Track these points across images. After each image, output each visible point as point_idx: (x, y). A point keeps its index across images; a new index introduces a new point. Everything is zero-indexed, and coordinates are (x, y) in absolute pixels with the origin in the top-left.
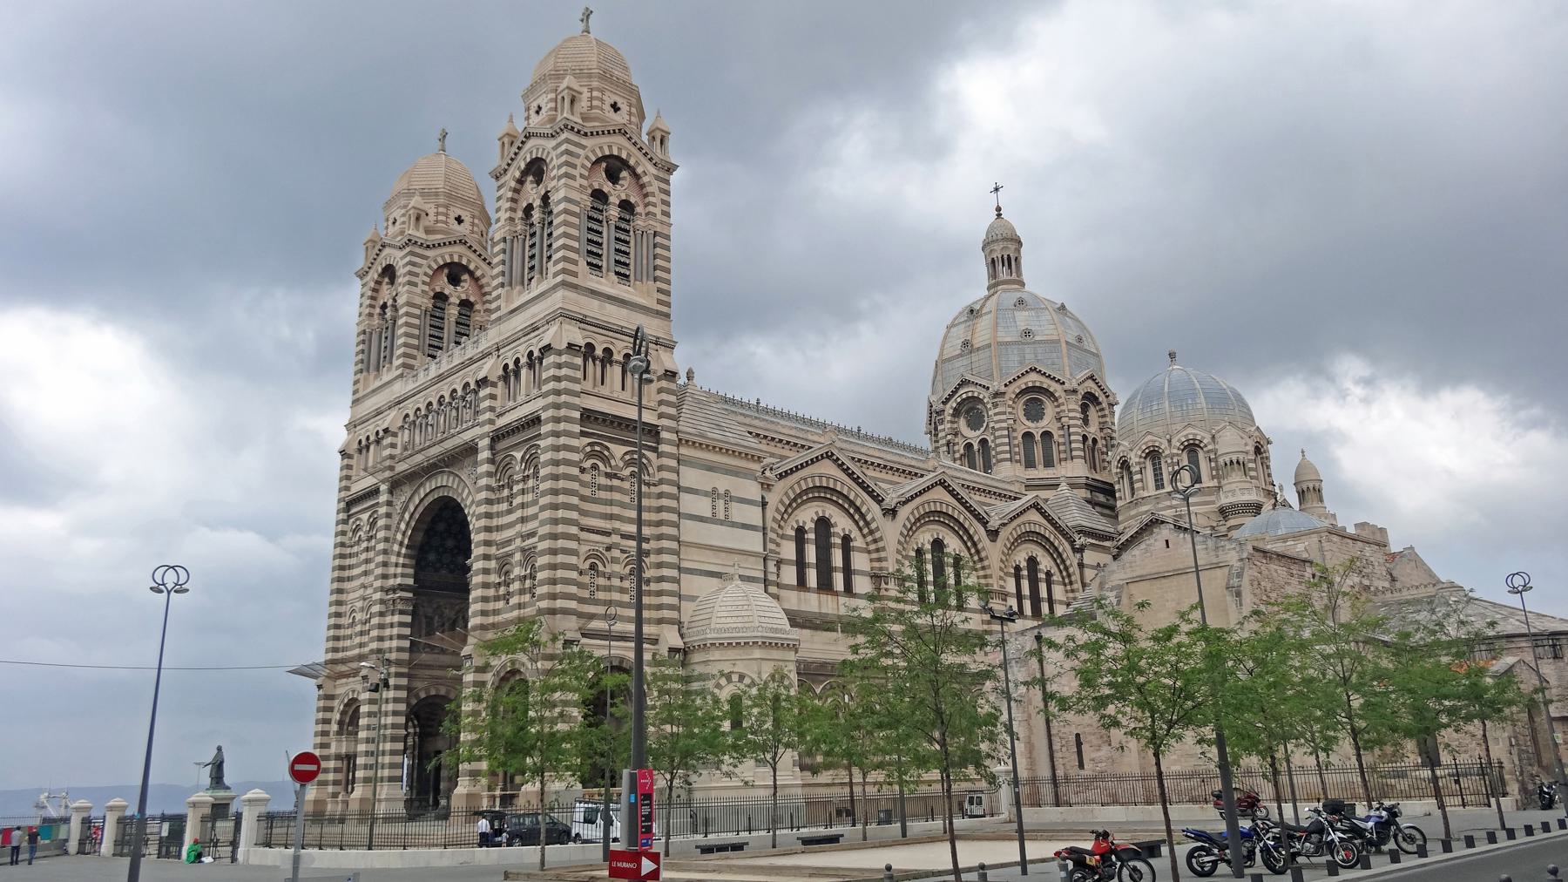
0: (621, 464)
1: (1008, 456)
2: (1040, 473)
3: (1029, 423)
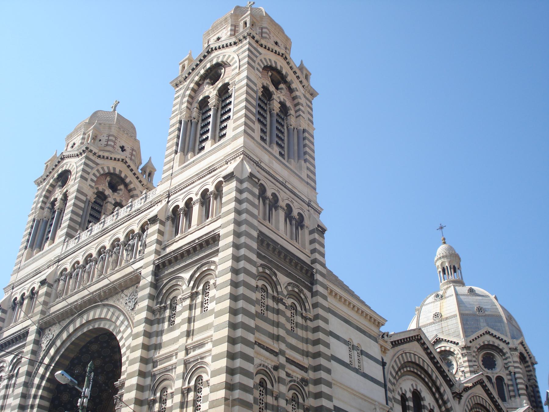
0: (285, 293)
3: (486, 370)
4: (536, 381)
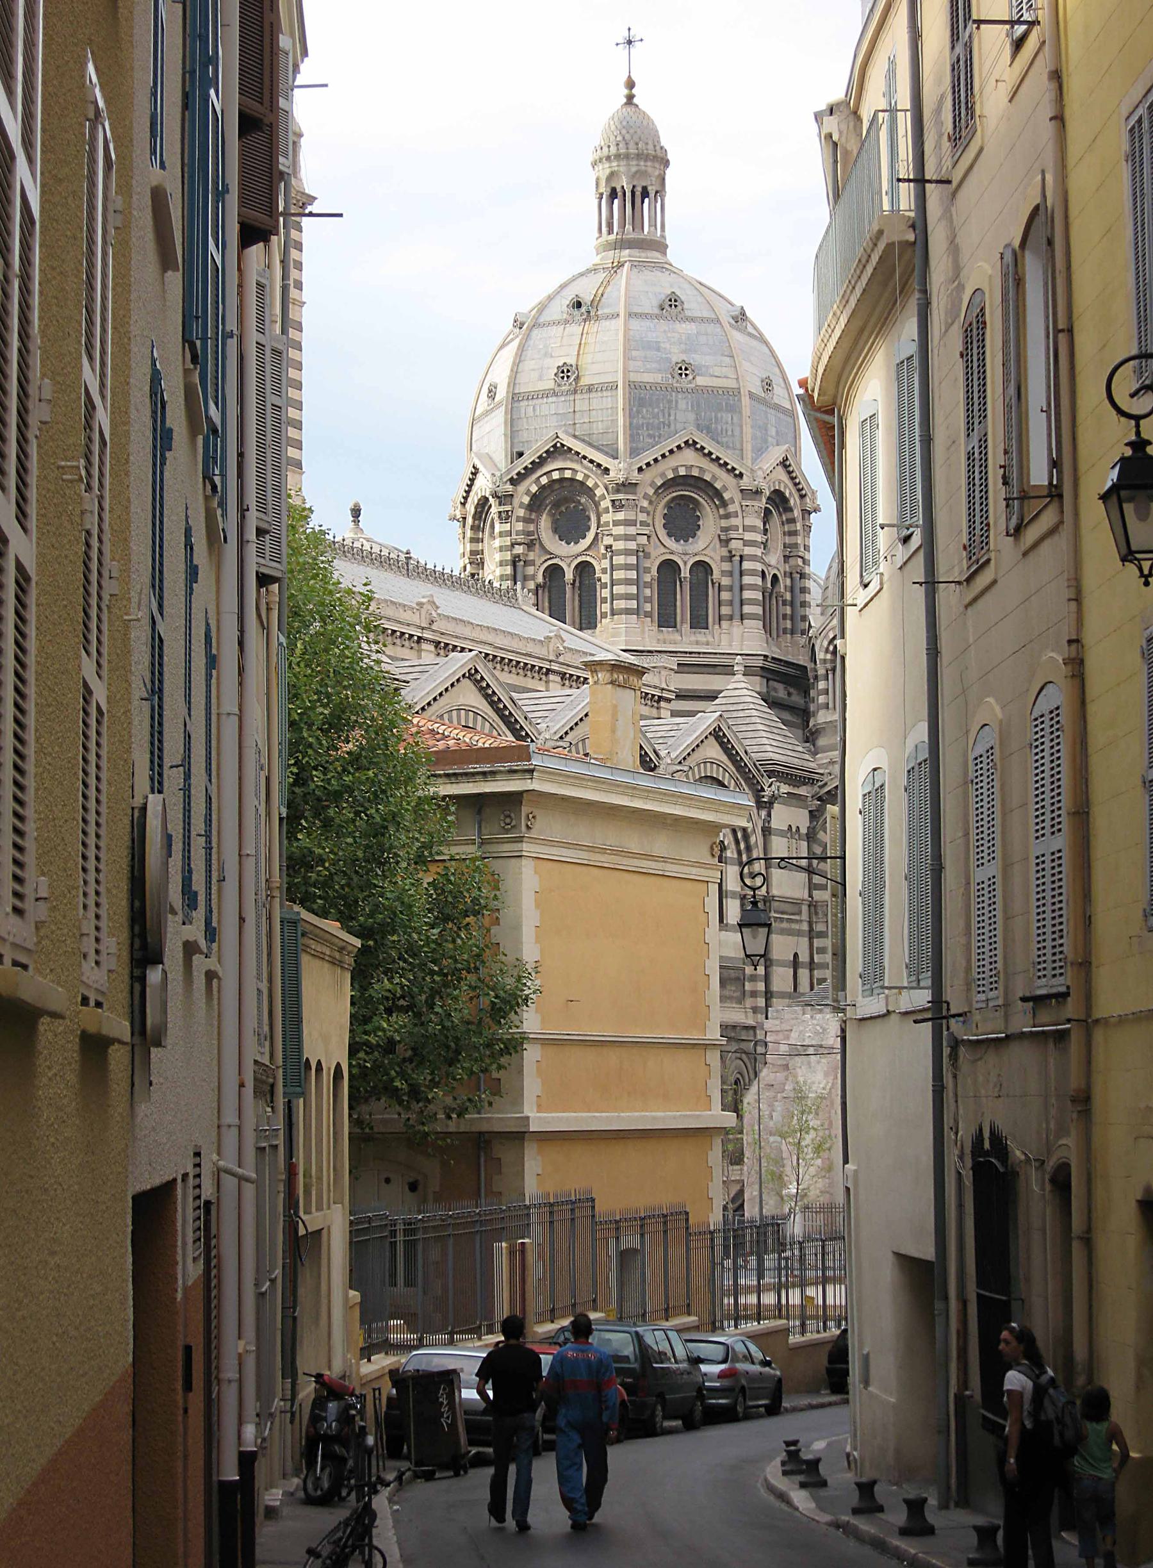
1: (633, 604)
2: (686, 640)
3: (670, 543)
4: (806, 562)
